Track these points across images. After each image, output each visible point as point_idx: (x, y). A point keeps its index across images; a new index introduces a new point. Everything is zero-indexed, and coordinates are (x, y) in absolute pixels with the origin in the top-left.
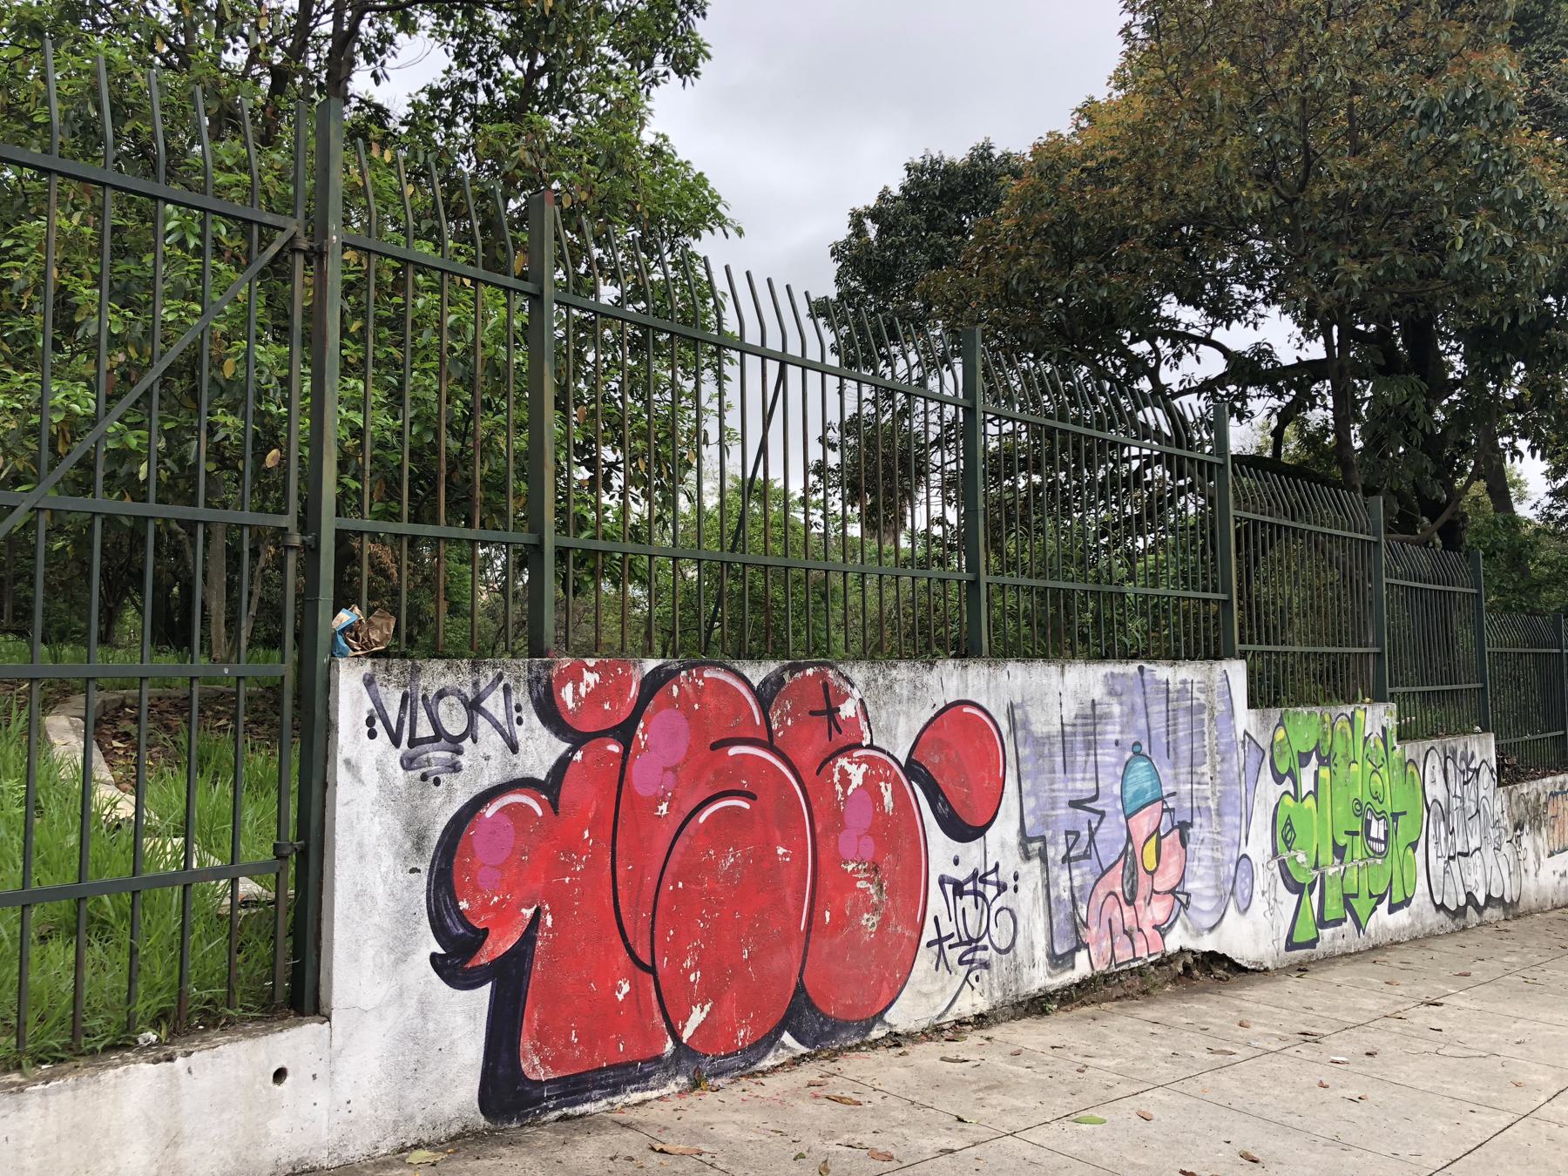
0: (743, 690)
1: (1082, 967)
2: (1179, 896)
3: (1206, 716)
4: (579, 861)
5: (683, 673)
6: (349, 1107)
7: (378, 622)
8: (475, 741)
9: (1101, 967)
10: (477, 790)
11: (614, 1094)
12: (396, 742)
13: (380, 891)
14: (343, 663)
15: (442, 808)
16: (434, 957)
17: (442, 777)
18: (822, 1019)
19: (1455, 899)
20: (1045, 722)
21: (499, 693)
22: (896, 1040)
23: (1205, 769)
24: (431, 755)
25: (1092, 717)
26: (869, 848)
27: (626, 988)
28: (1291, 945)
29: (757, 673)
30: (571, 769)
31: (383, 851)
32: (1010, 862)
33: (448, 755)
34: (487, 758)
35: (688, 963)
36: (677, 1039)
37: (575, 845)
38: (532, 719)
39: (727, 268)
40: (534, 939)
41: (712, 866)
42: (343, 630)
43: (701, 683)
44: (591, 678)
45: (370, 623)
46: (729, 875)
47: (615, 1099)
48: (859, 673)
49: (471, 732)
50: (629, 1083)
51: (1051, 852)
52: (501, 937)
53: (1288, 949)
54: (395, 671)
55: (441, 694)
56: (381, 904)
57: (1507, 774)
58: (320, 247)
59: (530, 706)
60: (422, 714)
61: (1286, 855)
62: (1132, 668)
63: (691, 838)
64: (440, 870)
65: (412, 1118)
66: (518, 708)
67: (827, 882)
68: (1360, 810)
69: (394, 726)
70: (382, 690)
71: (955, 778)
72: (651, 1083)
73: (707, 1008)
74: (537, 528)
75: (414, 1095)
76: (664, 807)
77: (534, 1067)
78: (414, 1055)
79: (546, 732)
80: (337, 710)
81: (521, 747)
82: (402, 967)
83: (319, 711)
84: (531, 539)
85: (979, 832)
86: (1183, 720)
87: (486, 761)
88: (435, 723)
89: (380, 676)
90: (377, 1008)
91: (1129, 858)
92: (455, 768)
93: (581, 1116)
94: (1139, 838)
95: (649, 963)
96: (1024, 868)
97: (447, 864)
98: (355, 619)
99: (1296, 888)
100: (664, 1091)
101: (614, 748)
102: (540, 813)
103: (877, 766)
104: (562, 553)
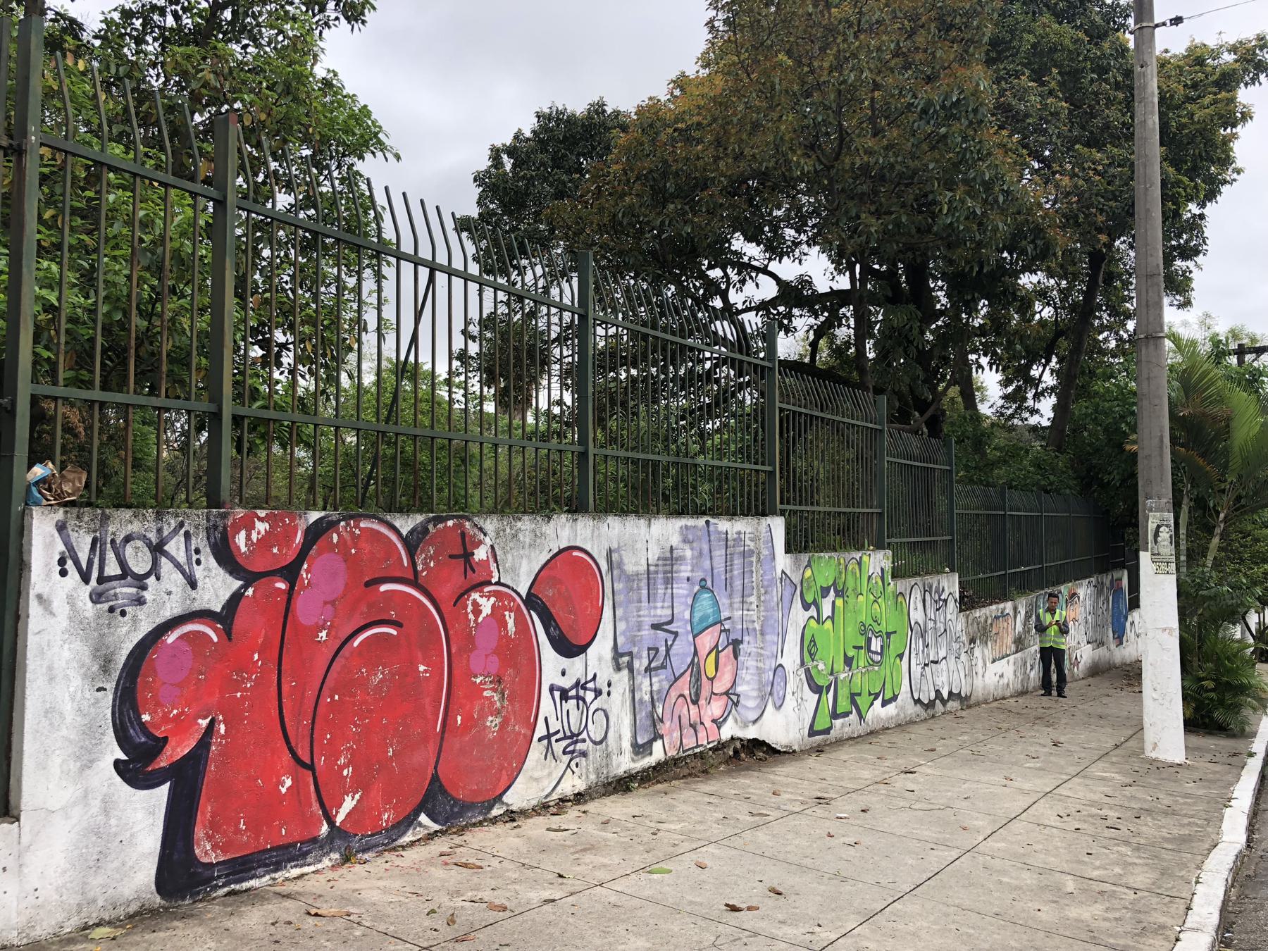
0: (394, 538)
1: (658, 753)
3: (754, 559)
4: (249, 679)
5: (342, 523)
6: (37, 894)
7: (71, 476)
8: (158, 579)
9: (672, 753)
10: (159, 621)
11: (276, 871)
12: (86, 578)
13: (68, 708)
14: (36, 511)
15: (127, 636)
16: (117, 763)
17: (128, 609)
18: (452, 803)
20: (634, 563)
21: (180, 538)
22: (512, 816)
23: (753, 599)
24: (118, 590)
25: (670, 559)
26: (494, 664)
27: (289, 783)
28: (812, 732)
29: (406, 524)
30: (243, 605)
31: (71, 673)
33: (134, 590)
34: (169, 593)
35: (342, 761)
36: (331, 823)
37: (247, 666)
38: (209, 561)
39: (386, 188)
40: (210, 744)
41: (363, 682)
42: (37, 483)
43: (357, 532)
44: (262, 527)
45: (62, 477)
46: (378, 688)
47: (277, 875)
48: (490, 525)
49: (155, 570)
50: (289, 861)
51: (636, 664)
52: (179, 744)
53: (810, 735)
54: (86, 519)
55: (128, 539)
56: (69, 719)
57: (967, 603)
58: (20, 146)
59: (208, 549)
60: (110, 556)
61: (810, 664)
62: (701, 522)
63: (347, 659)
64: (124, 689)
65: (94, 901)
66: (197, 551)
67: (459, 693)
68: (864, 630)
69: (84, 566)
70: (73, 535)
72: (309, 860)
73: (357, 796)
74: (216, 398)
75: (96, 881)
76: (323, 634)
77: (206, 852)
78: (100, 843)
79: (221, 571)
80: (30, 551)
81: (200, 584)
82: (88, 772)
83: (13, 553)
84: (212, 408)
85: (582, 649)
86: (737, 562)
87: (167, 597)
88: (122, 563)
89: (71, 523)
90: (62, 809)
91: (695, 668)
92: (140, 601)
93: (246, 891)
95: (308, 762)
96: (615, 677)
98: (48, 472)
99: (817, 689)
100: (319, 866)
101: (281, 585)
102: (215, 639)
104: (237, 420)
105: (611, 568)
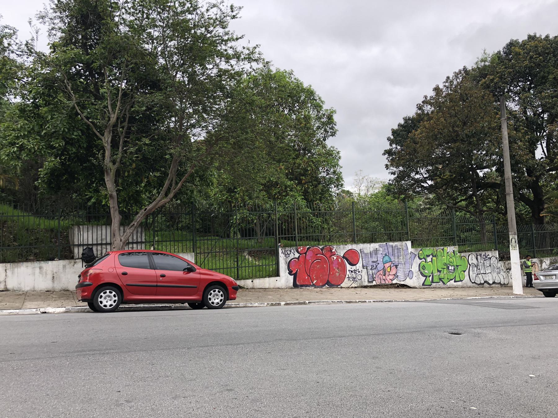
1: (374, 283)
2: (396, 276)
9: (378, 284)
22: (342, 288)
23: (402, 257)
26: (337, 266)
28: (423, 284)
32: (361, 269)
61: (422, 271)
62: (385, 243)
67: (331, 269)
71: (352, 258)
77: (298, 283)
78: (287, 281)
85: (355, 265)
87: (292, 256)
91: (384, 269)
96: (363, 270)
97: (289, 265)
103: (338, 257)
105: (361, 252)
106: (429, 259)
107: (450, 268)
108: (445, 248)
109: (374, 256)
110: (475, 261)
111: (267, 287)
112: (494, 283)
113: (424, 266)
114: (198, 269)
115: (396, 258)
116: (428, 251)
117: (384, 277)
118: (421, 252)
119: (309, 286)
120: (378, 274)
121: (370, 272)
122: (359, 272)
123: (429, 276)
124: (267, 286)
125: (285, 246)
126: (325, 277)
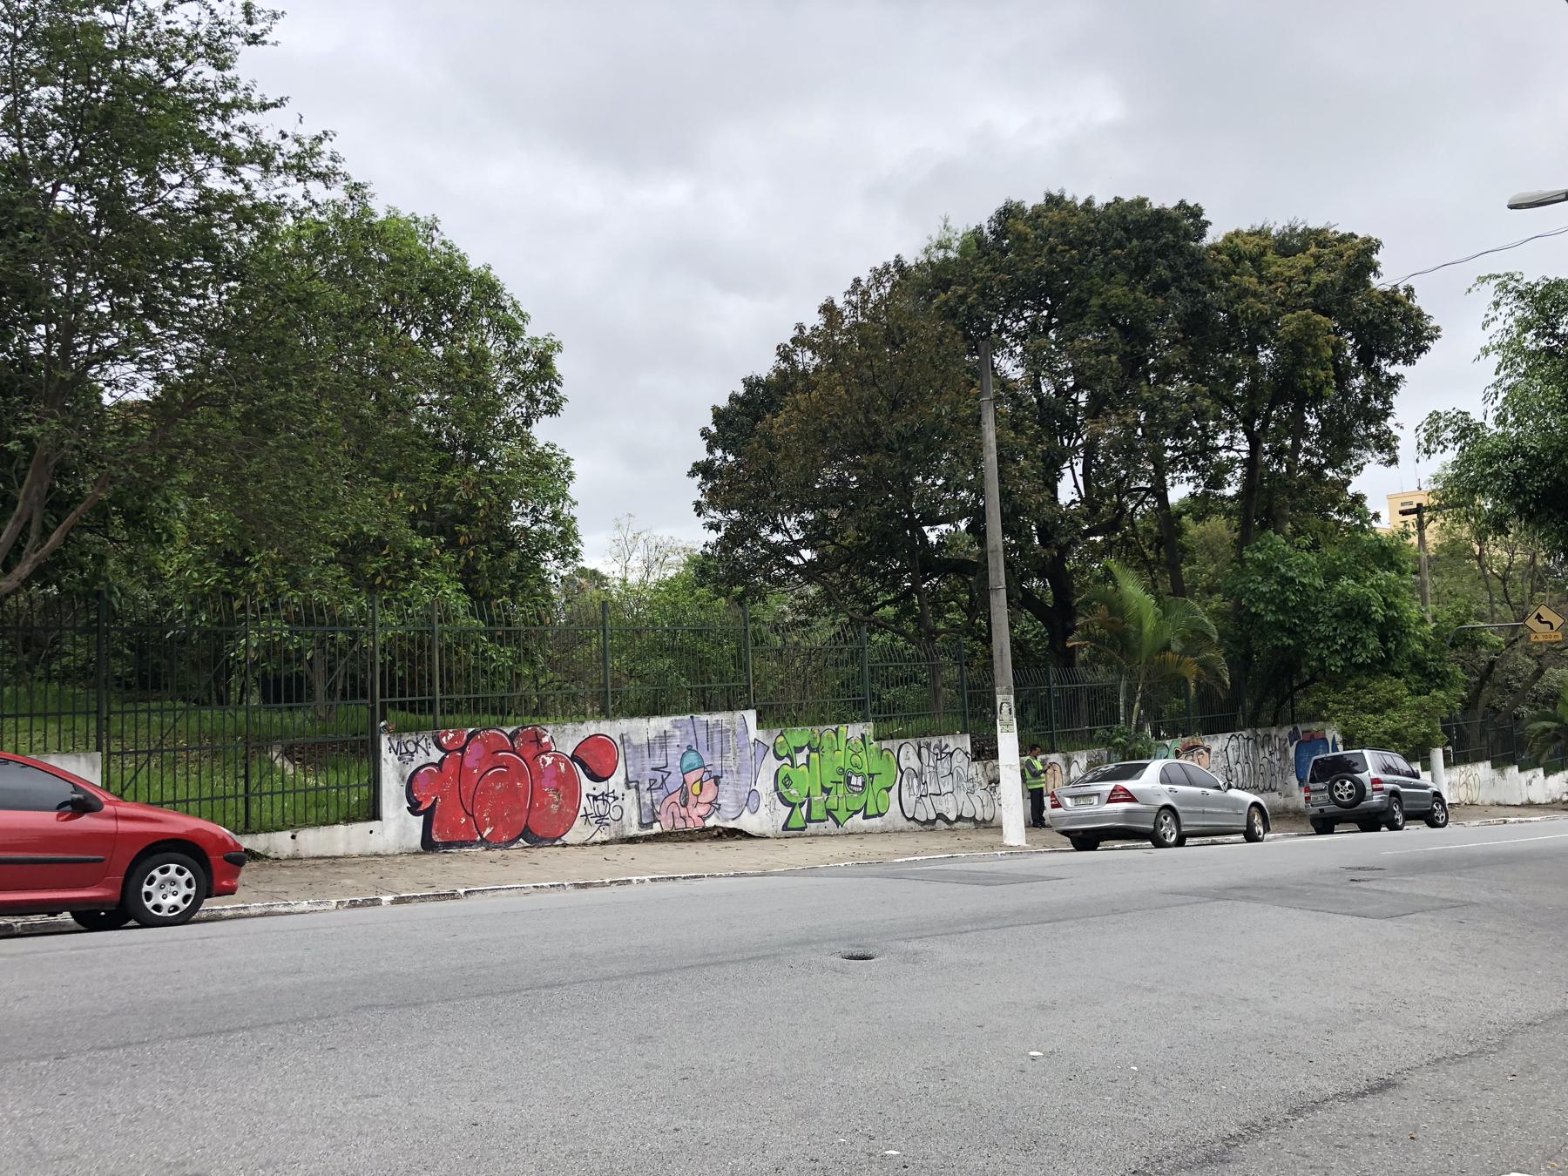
1: (657, 828)
2: (714, 806)
15: (409, 771)
18: (534, 837)
19: (925, 812)
22: (565, 845)
26: (554, 783)
28: (785, 827)
37: (447, 781)
61: (782, 789)
62: (687, 717)
67: (537, 794)
71: (596, 760)
77: (436, 838)
78: (404, 831)
85: (606, 779)
86: (717, 737)
87: (420, 759)
91: (684, 790)
94: (689, 783)
96: (627, 792)
103: (558, 757)
105: (623, 742)
106: (801, 758)
107: (854, 781)
108: (842, 728)
109: (658, 751)
110: (914, 763)
111: (340, 853)
112: (960, 818)
113: (787, 776)
114: (109, 802)
115: (717, 755)
116: (799, 736)
117: (683, 811)
118: (781, 739)
119: (470, 846)
120: (668, 801)
121: (647, 798)
122: (616, 798)
123: (801, 805)
124: (340, 850)
125: (400, 730)
126: (518, 818)
